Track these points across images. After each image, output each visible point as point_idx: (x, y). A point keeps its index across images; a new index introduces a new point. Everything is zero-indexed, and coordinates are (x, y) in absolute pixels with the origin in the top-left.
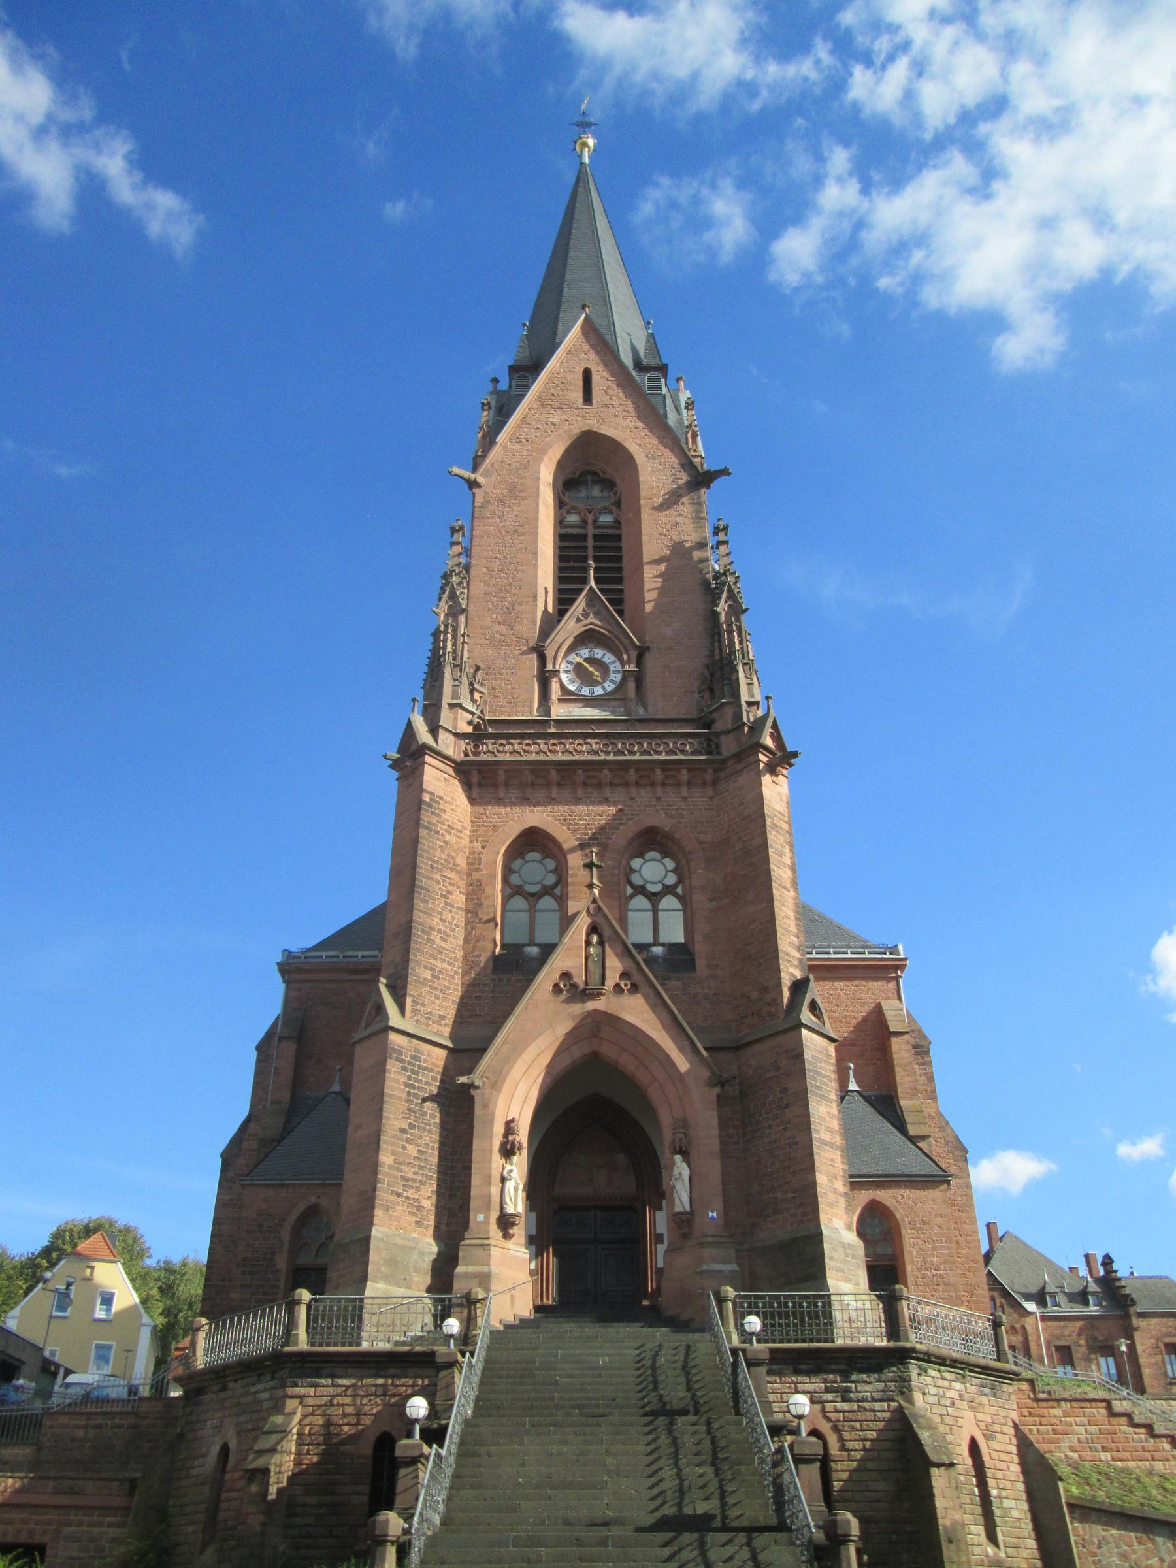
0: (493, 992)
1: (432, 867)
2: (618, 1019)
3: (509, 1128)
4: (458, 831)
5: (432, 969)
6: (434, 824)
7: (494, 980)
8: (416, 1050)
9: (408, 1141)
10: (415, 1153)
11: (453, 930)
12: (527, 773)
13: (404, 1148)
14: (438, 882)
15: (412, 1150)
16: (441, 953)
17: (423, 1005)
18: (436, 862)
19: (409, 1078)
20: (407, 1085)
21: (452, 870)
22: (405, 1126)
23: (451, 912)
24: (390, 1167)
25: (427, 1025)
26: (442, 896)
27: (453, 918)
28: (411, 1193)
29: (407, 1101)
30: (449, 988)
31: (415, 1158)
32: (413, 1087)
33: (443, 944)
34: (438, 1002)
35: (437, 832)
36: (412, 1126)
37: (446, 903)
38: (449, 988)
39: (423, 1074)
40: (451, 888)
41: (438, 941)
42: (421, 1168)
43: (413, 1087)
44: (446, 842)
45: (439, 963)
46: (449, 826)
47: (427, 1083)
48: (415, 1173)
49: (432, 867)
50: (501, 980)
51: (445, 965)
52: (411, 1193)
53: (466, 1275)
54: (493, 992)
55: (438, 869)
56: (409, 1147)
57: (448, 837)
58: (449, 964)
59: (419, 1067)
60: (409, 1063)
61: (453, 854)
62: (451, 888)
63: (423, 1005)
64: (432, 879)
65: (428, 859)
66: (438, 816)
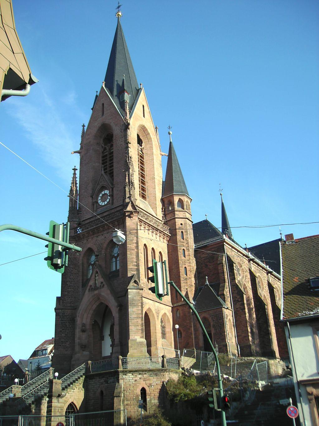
3: (84, 325)
8: (63, 312)
12: (86, 234)
16: (70, 287)
17: (66, 301)
39: (66, 317)
45: (70, 289)
50: (83, 289)
58: (72, 288)
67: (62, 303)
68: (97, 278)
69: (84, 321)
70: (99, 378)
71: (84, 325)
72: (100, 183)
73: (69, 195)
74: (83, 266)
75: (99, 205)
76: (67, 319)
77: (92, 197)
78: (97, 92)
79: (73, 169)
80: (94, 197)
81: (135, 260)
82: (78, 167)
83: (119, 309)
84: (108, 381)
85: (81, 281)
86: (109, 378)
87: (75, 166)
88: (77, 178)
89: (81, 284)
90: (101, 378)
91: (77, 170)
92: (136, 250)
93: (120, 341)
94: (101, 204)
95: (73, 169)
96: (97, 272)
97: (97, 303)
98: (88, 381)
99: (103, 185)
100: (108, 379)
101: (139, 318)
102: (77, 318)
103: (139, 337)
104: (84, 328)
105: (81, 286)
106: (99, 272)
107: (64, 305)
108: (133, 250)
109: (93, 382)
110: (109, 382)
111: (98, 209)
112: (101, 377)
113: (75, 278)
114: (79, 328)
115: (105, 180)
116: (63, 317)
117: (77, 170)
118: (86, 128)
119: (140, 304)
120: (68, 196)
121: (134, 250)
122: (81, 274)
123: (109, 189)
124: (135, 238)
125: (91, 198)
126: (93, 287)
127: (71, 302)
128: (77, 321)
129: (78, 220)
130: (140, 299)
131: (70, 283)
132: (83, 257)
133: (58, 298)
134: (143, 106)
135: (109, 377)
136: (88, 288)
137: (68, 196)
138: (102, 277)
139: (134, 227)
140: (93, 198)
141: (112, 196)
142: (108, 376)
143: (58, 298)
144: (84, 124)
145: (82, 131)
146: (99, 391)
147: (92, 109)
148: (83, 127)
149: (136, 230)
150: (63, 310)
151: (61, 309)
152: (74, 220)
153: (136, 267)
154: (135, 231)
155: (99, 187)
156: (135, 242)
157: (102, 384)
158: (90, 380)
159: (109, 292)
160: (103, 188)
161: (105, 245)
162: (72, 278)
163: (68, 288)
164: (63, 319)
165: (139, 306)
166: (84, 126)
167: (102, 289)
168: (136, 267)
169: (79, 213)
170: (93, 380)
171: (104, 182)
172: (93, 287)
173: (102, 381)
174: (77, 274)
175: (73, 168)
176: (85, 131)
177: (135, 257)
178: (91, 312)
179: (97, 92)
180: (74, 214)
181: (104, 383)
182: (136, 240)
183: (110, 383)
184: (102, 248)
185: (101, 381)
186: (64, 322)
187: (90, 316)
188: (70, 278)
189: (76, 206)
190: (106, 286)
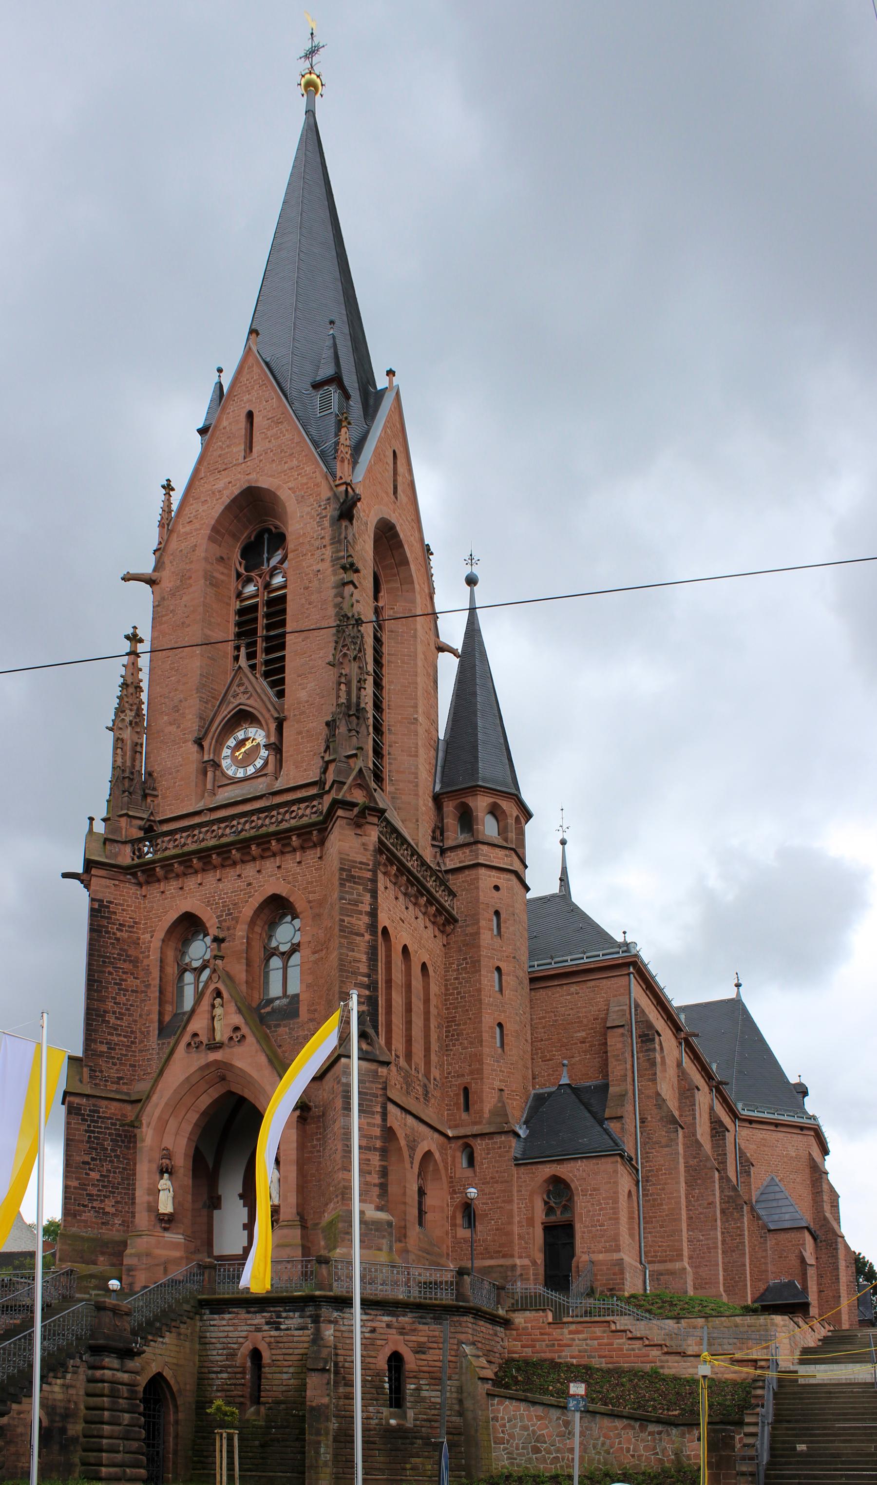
0: (158, 1054)
1: (104, 962)
2: (231, 1065)
4: (130, 927)
5: (107, 1043)
6: (104, 926)
7: (159, 1044)
8: (94, 1105)
9: (90, 1169)
10: (98, 1177)
11: (128, 1009)
13: (88, 1174)
14: (110, 973)
15: (94, 1175)
16: (116, 1029)
17: (101, 1071)
18: (109, 957)
19: (89, 1126)
20: (86, 1131)
21: (125, 961)
22: (87, 1159)
23: (125, 995)
24: (75, 1188)
25: (106, 1086)
26: (115, 984)
27: (128, 1000)
28: (95, 1204)
29: (88, 1142)
30: (126, 1055)
31: (98, 1180)
32: (93, 1132)
33: (119, 1022)
34: (115, 1067)
35: (107, 932)
36: (93, 1159)
37: (119, 989)
38: (126, 1055)
40: (124, 976)
41: (113, 1020)
42: (103, 1186)
43: (93, 1132)
44: (118, 939)
45: (115, 1038)
46: (120, 925)
47: (108, 1128)
48: (98, 1191)
49: (104, 962)
50: (163, 1044)
51: (122, 1039)
52: (95, 1204)
53: (131, 1255)
54: (158, 1054)
55: (110, 963)
56: (92, 1174)
57: (119, 934)
58: (125, 1036)
59: (99, 1117)
60: (88, 1115)
61: (126, 947)
62: (124, 976)
63: (101, 1071)
64: (105, 972)
65: (99, 956)
66: (110, 918)
67: (91, 1077)
68: (218, 1011)
69: (168, 1142)
70: (248, 1312)
71: (168, 1154)
72: (232, 699)
73: (110, 725)
74: (162, 969)
75: (224, 774)
76: (105, 1128)
77: (199, 742)
78: (220, 370)
79: (127, 637)
80: (206, 744)
81: (364, 969)
82: (145, 633)
83: (299, 1117)
84: (280, 1323)
85: (155, 1017)
86: (284, 1314)
87: (135, 628)
88: (141, 670)
89: (156, 1025)
90: (255, 1312)
91: (141, 641)
92: (367, 937)
93: (298, 1214)
94: (230, 773)
95: (127, 637)
96: (219, 994)
97: (214, 1093)
98: (205, 1317)
99: (241, 707)
100: (279, 1317)
101: (375, 1149)
102: (144, 1129)
103: (372, 1206)
104: (167, 1161)
105: (157, 1032)
106: (225, 994)
107: (96, 1084)
108: (357, 934)
109: (224, 1323)
110: (282, 1327)
111: (219, 787)
112: (252, 1309)
113: (131, 1005)
114: (150, 1161)
115: (250, 689)
116: (92, 1121)
117: (141, 641)
118: (176, 498)
119: (379, 1109)
120: (107, 728)
121: (363, 936)
122: (154, 993)
123: (267, 724)
124: (367, 898)
125: (195, 748)
126: (204, 1038)
127: (120, 1078)
128: (143, 1141)
129: (145, 816)
130: (380, 1092)
131: (117, 1018)
132: (163, 941)
133: (72, 1060)
134: (394, 452)
135: (286, 1311)
136: (186, 1038)
137: (107, 728)
138: (239, 1011)
139: (365, 861)
140: (201, 747)
141: (276, 748)
142: (281, 1309)
143: (72, 1060)
144: (168, 480)
145: (162, 504)
146: (248, 1346)
147: (202, 431)
148: (164, 492)
149: (369, 870)
150: (92, 1101)
151: (88, 1096)
152: (131, 813)
153: (367, 993)
154: (369, 875)
155: (226, 712)
156: (368, 908)
157: (259, 1330)
158: (211, 1313)
159: (263, 1059)
160: (243, 717)
161: (248, 911)
162: (124, 1004)
163: (111, 1034)
164: (94, 1127)
165: (373, 1113)
166: (168, 488)
167: (238, 1050)
168: (367, 993)
169: (147, 791)
170: (227, 1316)
171: (246, 696)
172: (204, 1038)
173: (259, 1319)
174: (142, 992)
175: (130, 631)
176: (174, 507)
177: (364, 958)
178: (193, 1117)
179: (220, 370)
180: (130, 793)
181: (266, 1327)
182: (371, 905)
183: (287, 1329)
184: (236, 920)
185: (255, 1322)
186: (95, 1137)
187: (188, 1128)
188: (115, 1003)
189: (137, 768)
190: (250, 1039)
